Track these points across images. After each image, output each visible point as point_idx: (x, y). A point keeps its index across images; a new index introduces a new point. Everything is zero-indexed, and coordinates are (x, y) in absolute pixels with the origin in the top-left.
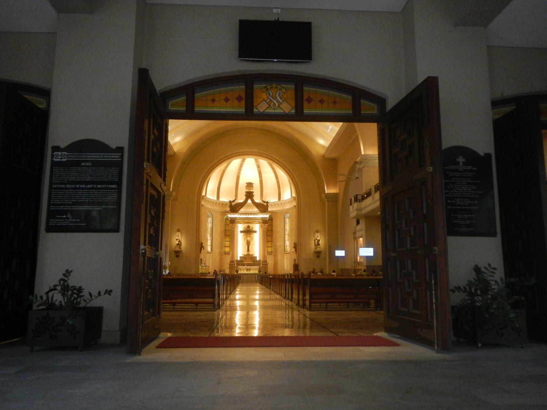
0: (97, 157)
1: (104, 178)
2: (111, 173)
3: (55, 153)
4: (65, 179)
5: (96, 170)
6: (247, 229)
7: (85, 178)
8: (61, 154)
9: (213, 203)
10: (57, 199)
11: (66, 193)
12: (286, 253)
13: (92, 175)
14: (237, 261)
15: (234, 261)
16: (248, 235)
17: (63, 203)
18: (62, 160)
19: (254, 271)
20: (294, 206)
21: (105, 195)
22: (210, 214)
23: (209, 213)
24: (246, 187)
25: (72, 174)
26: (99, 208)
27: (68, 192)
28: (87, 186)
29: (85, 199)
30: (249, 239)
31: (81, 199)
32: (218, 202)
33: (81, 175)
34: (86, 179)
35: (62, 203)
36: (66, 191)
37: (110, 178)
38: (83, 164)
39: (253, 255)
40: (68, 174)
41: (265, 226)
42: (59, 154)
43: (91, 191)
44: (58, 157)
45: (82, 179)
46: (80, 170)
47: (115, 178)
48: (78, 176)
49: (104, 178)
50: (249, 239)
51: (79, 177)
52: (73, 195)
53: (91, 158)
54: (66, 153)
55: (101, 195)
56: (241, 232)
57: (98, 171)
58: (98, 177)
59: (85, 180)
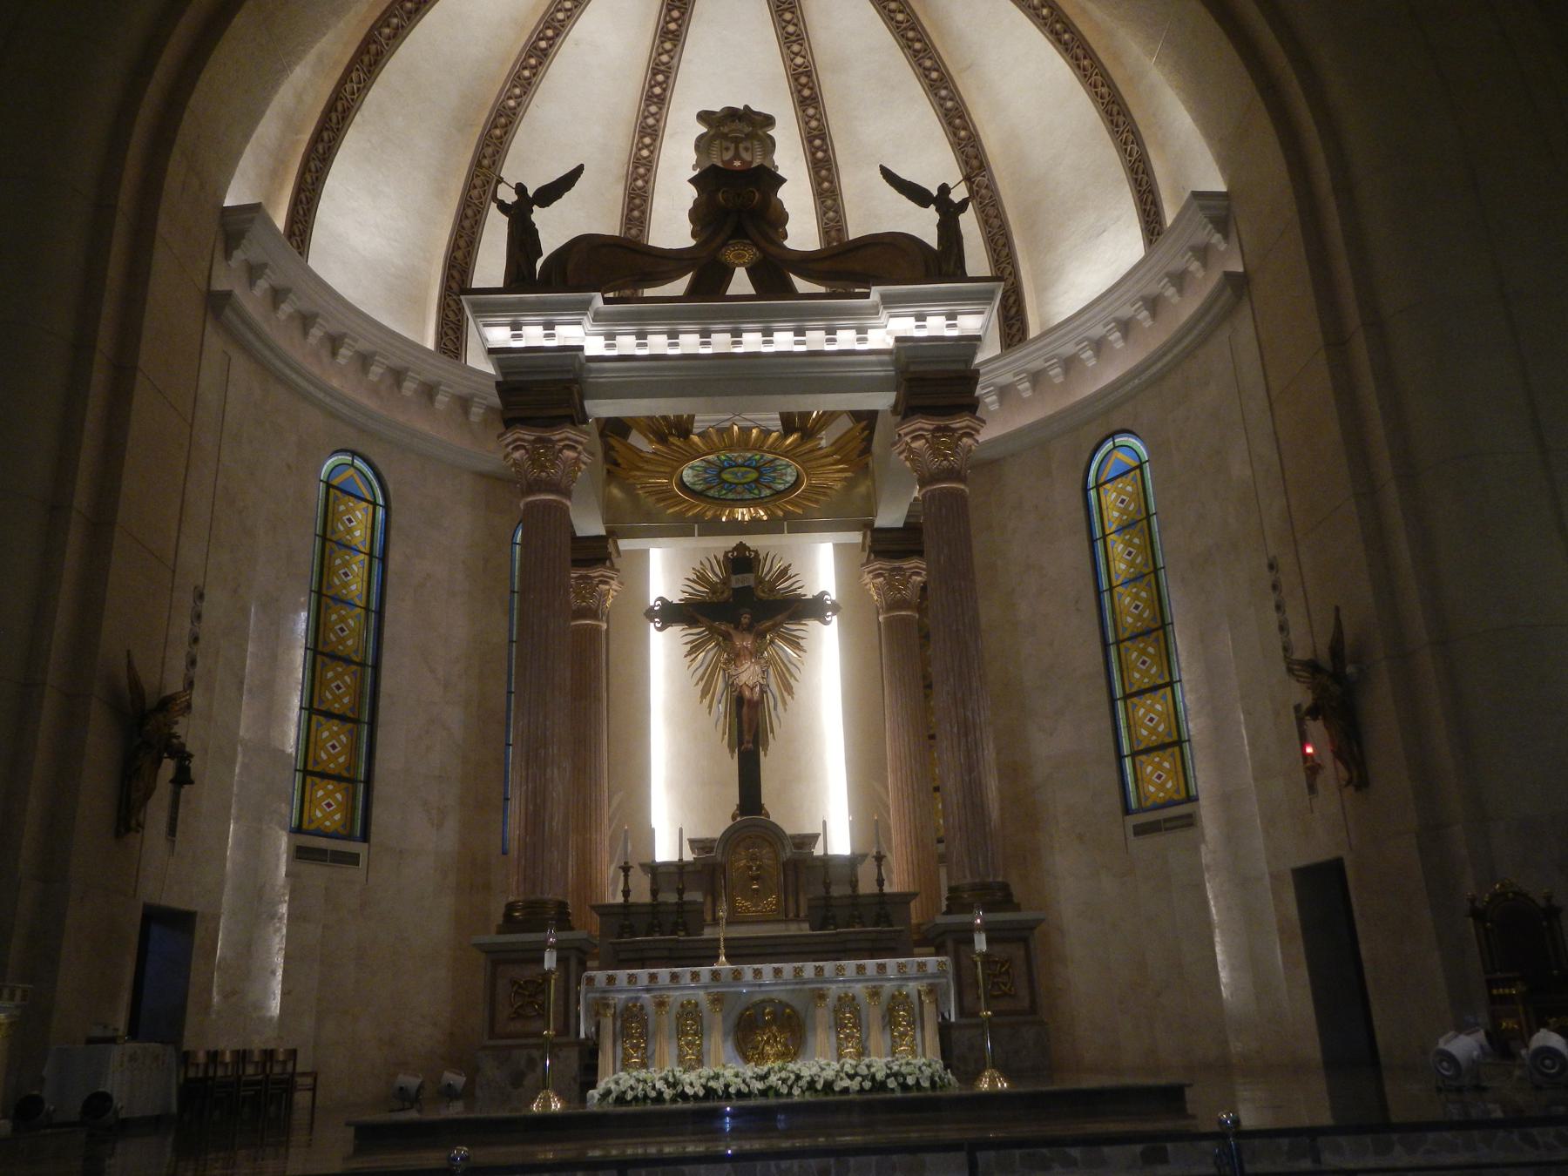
6: (725, 582)
9: (398, 376)
12: (1140, 830)
14: (623, 917)
15: (562, 905)
16: (745, 642)
19: (862, 1053)
20: (1229, 276)
22: (358, 463)
23: (347, 459)
24: (697, 147)
30: (748, 673)
32: (441, 370)
39: (815, 837)
41: (954, 446)
50: (748, 673)
56: (670, 614)
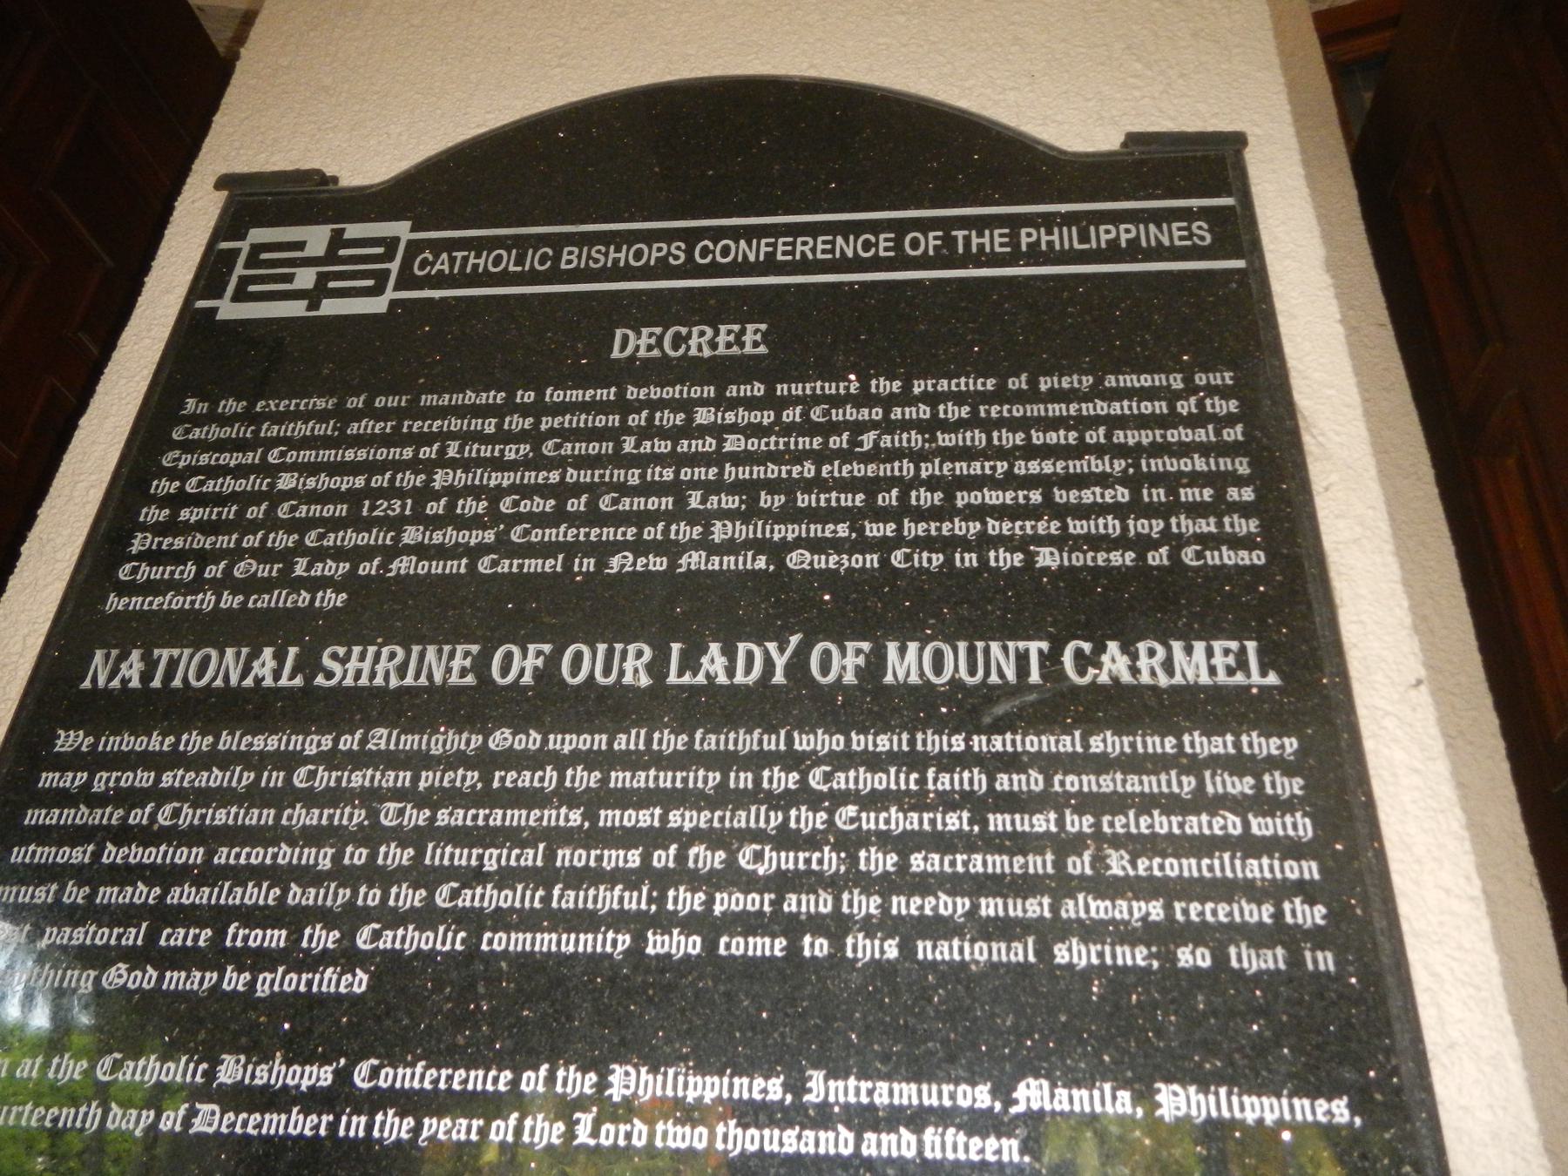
0: (847, 247)
1: (994, 526)
2: (1121, 451)
3: (258, 235)
4: (318, 555)
5: (851, 413)
7: (651, 533)
8: (337, 240)
10: (108, 894)
11: (284, 798)
13: (787, 487)
17: (197, 981)
18: (330, 307)
21: (1043, 823)
25: (440, 479)
26: (944, 1117)
27: (325, 779)
28: (690, 662)
29: (636, 901)
31: (566, 899)
33: (594, 490)
34: (672, 549)
35: (175, 980)
36: (288, 761)
37: (1111, 526)
38: (634, 343)
40: (379, 481)
42: (300, 246)
43: (757, 761)
44: (289, 278)
45: (603, 551)
46: (582, 420)
47: (1207, 526)
48: (540, 505)
49: (994, 526)
51: (559, 517)
52: (417, 817)
53: (770, 265)
54: (401, 230)
55: (955, 822)
57: (888, 426)
58: (882, 515)
59: (658, 564)
